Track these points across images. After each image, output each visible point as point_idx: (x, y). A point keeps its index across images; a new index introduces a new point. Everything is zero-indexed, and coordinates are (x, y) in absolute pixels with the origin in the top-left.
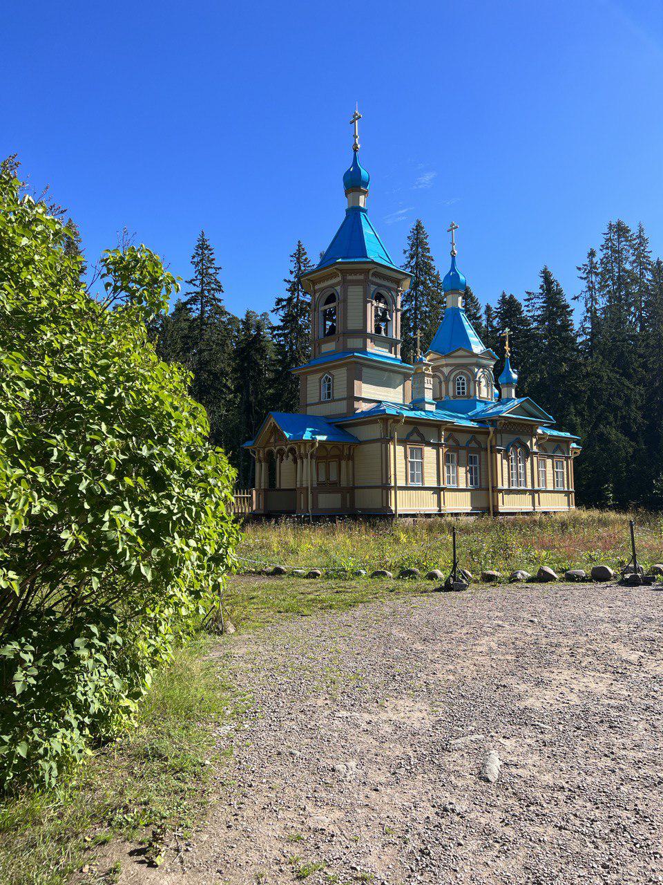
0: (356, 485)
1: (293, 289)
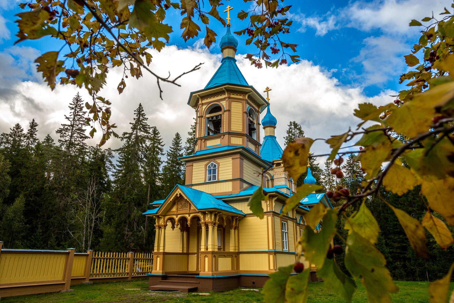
0: (241, 250)
1: (134, 128)
